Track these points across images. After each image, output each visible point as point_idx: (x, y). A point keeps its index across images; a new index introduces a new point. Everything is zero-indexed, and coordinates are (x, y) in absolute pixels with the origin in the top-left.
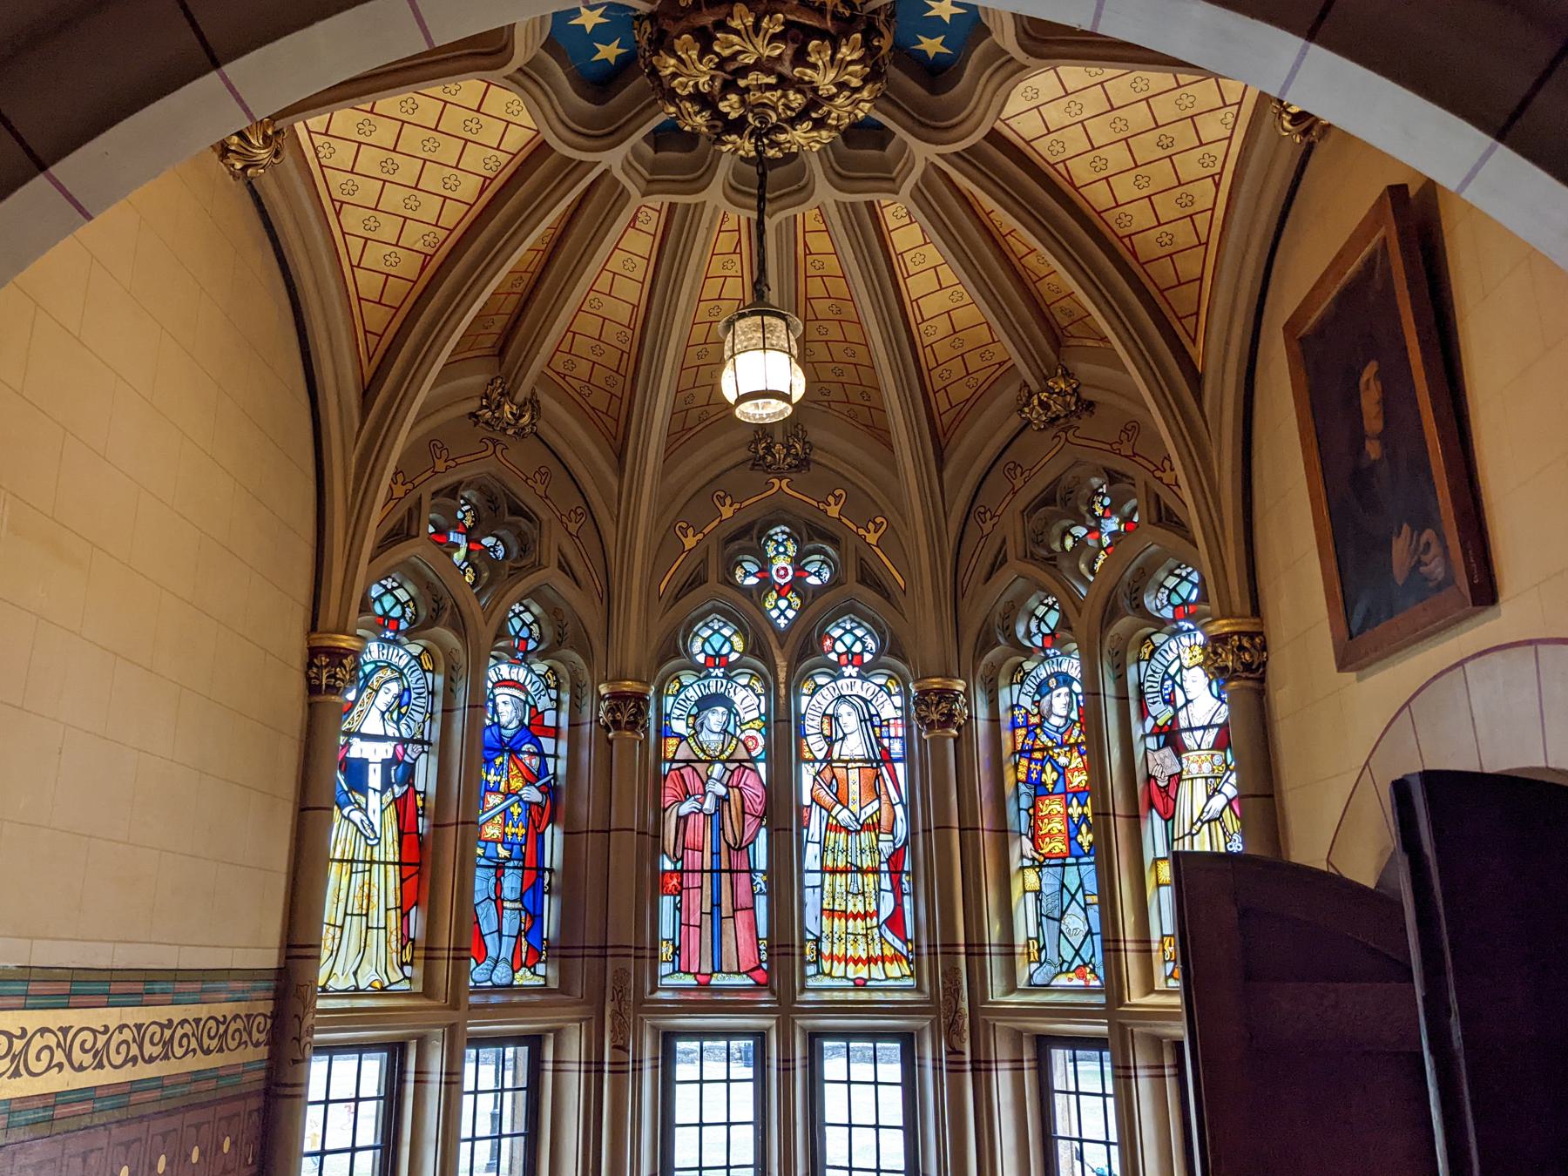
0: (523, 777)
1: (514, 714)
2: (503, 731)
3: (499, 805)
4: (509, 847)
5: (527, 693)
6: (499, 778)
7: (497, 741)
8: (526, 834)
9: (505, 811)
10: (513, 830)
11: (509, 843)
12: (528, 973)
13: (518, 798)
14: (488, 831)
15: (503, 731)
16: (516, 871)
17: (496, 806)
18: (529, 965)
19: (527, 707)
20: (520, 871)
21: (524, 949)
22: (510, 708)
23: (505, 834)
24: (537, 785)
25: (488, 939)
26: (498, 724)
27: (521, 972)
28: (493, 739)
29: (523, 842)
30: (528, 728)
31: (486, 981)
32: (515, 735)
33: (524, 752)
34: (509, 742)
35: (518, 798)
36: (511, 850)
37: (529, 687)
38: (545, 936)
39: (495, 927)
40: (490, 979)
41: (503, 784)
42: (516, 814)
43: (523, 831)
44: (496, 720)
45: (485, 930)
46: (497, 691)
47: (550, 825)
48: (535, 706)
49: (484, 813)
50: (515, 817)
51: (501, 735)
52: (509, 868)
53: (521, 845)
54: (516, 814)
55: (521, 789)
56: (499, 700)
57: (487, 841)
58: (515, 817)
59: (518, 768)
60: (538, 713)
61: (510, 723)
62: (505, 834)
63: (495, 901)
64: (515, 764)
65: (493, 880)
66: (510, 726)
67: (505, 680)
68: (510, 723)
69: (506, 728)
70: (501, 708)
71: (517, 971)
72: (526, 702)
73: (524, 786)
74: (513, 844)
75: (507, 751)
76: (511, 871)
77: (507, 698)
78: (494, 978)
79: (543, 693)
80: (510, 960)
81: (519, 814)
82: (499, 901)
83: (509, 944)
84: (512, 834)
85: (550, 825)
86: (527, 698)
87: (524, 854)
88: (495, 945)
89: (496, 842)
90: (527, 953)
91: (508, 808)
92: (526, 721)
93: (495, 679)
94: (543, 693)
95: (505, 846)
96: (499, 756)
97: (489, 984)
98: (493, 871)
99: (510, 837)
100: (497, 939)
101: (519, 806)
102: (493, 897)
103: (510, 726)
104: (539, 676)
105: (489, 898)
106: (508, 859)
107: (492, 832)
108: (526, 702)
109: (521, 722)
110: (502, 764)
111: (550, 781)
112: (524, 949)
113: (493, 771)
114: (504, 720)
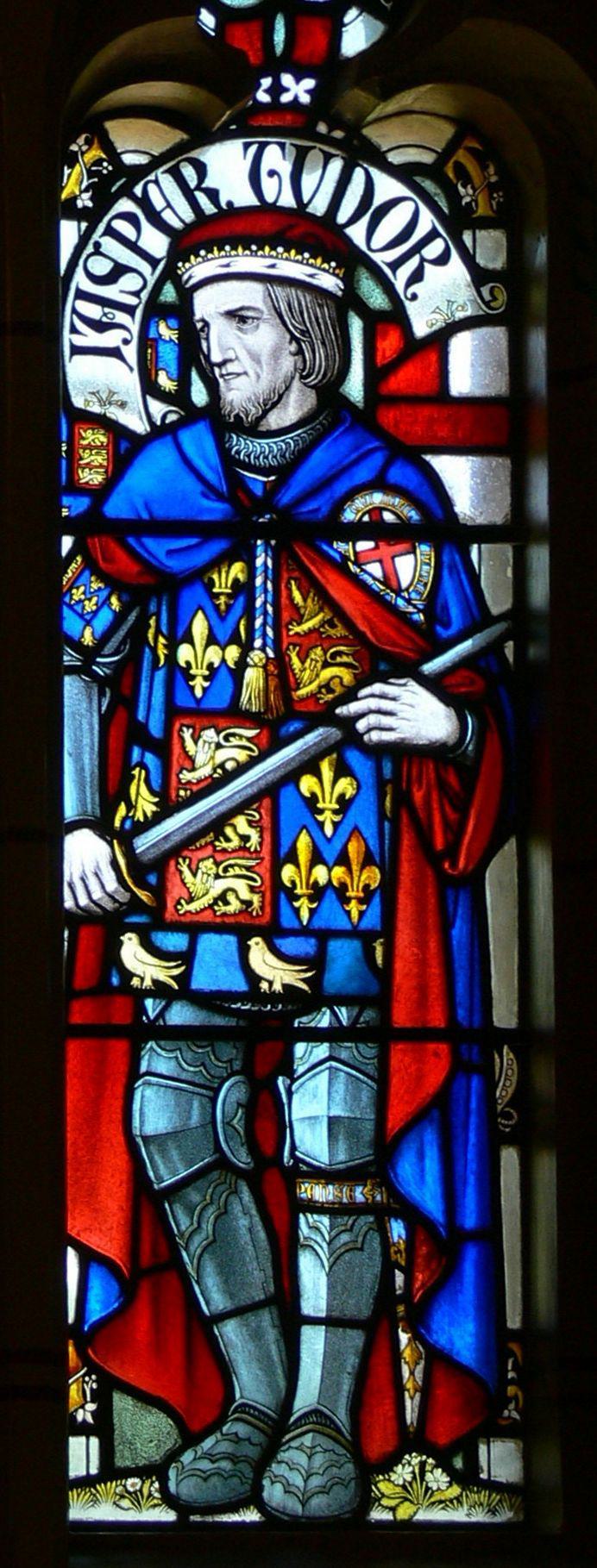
0: (356, 637)
1: (288, 363)
2: (243, 446)
3: (242, 769)
4: (305, 946)
5: (350, 260)
6: (233, 653)
7: (210, 490)
8: (389, 888)
9: (271, 793)
10: (320, 874)
11: (304, 932)
12: (437, 1478)
13: (334, 733)
14: (195, 883)
15: (243, 446)
16: (347, 1050)
17: (228, 777)
18: (442, 1438)
19: (356, 326)
20: (369, 1050)
21: (411, 1374)
22: (266, 336)
23: (279, 892)
24: (430, 667)
25: (231, 1333)
26: (216, 418)
27: (402, 1473)
28: (190, 484)
29: (373, 919)
30: (363, 419)
31: (234, 1507)
32: (302, 455)
33: (355, 532)
34: (272, 491)
35: (334, 733)
36: (317, 963)
37: (357, 233)
38: (514, 1321)
39: (258, 1279)
40: (255, 1498)
41: (253, 677)
42: (328, 803)
43: (373, 876)
44: (199, 395)
45: (212, 1295)
46: (198, 269)
47: (511, 846)
48: (397, 316)
49: (167, 808)
50: (328, 818)
51: (229, 461)
52: (315, 1036)
53: (366, 938)
54: (328, 803)
55: (350, 695)
56: (207, 304)
57: (194, 929)
58: (328, 818)
59: (326, 601)
60: (413, 348)
61: (274, 401)
62: (279, 892)
63: (254, 1179)
64: (312, 585)
65: (231, 1093)
66: (275, 420)
67: (232, 212)
68: (274, 401)
69: (253, 429)
70: (221, 341)
71: (387, 1465)
72: (350, 300)
73: (363, 681)
74: (323, 936)
75: (265, 532)
76: (322, 1050)
77: (251, 295)
78: (274, 1494)
79: (434, 249)
80: (342, 1416)
81: (344, 804)
82: (273, 1181)
83: (331, 1357)
84: (318, 893)
85: (511, 846)
86: (349, 281)
87: (384, 976)
88: (264, 1360)
89: (241, 929)
90: (426, 1390)
91: (291, 777)
92: (354, 387)
93: (180, 213)
94: (434, 249)
95: (289, 945)
96: (226, 559)
97: (251, 1516)
98: (228, 1051)
99: (304, 906)
100: (272, 1335)
101: (342, 770)
102: (242, 1159)
103: (275, 420)
104: (404, 173)
105: (222, 1163)
106: (314, 999)
107: (219, 887)
108: (350, 300)
109: (329, 392)
110: (244, 590)
111: (495, 648)
112: (411, 1374)
113: (200, 627)
114: (239, 394)
